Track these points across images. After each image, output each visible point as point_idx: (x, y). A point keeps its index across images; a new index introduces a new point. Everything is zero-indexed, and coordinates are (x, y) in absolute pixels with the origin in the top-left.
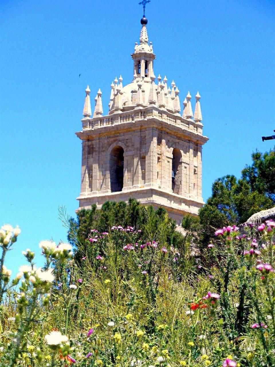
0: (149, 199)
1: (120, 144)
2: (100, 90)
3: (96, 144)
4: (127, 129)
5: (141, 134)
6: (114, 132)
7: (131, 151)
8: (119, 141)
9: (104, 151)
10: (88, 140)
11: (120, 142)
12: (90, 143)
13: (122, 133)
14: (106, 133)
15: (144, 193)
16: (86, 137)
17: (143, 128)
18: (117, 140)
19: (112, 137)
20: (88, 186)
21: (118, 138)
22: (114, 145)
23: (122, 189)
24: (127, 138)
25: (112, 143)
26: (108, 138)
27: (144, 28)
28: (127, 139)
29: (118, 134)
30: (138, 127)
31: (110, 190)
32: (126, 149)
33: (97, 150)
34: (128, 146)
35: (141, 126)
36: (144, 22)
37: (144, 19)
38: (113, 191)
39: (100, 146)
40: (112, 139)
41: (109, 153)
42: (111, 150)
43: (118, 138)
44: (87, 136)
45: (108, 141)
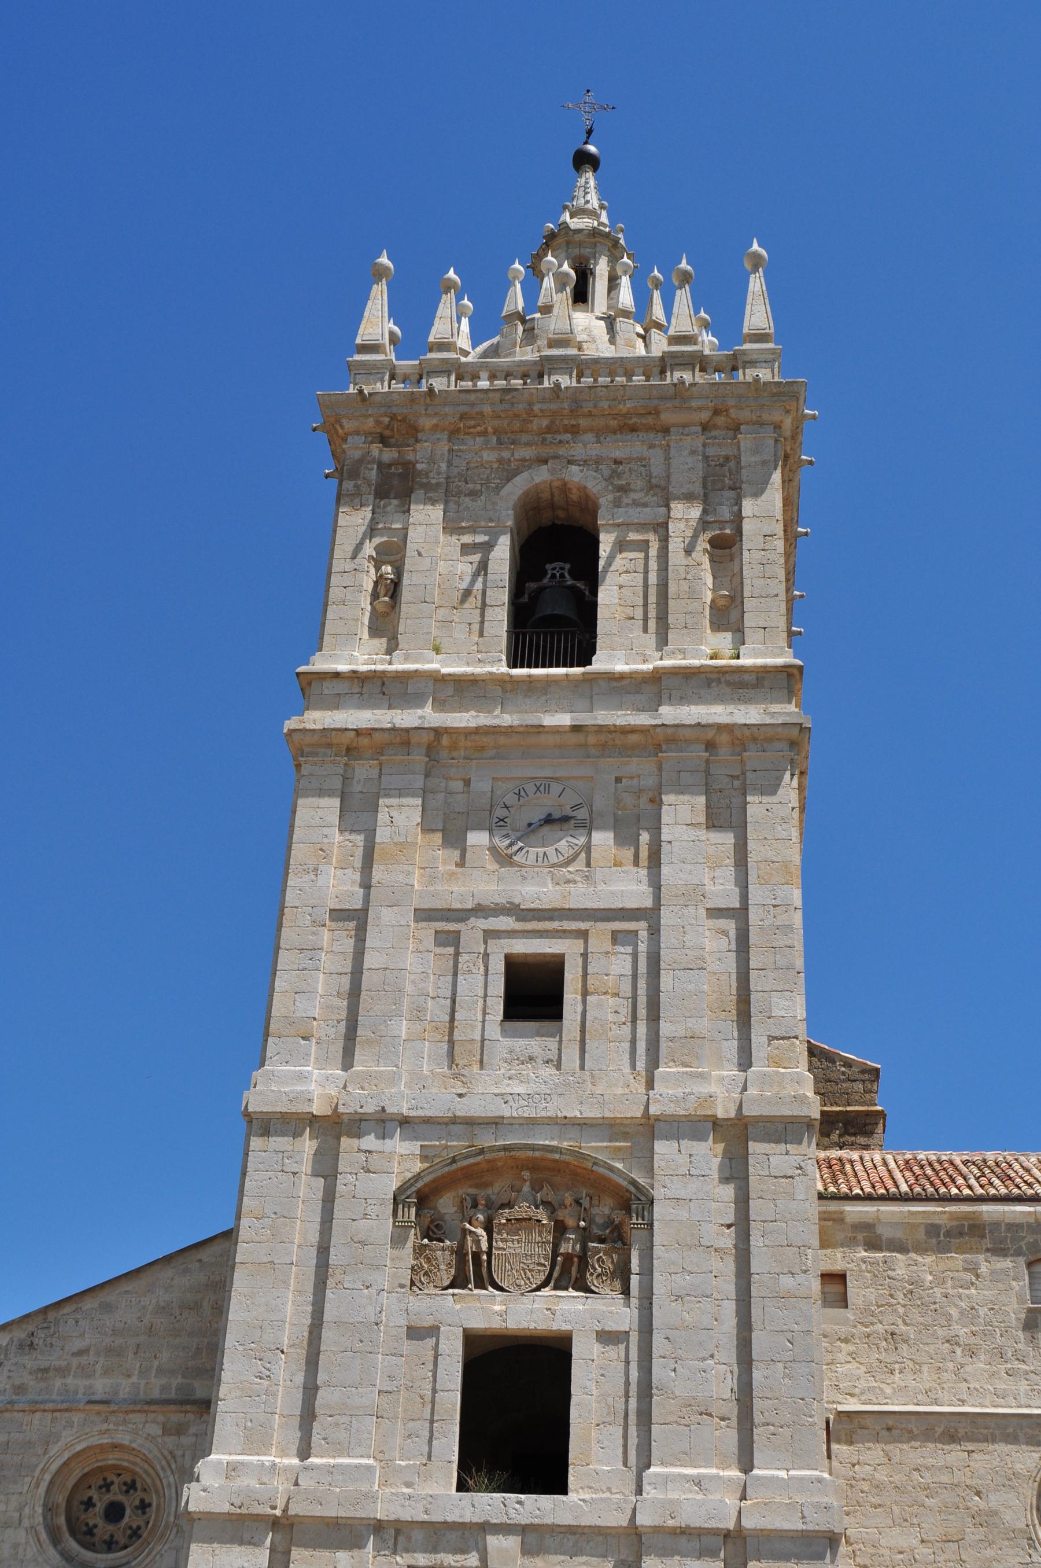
0: (776, 708)
1: (575, 475)
2: (452, 269)
3: (432, 460)
4: (628, 415)
5: (704, 445)
6: (545, 422)
7: (645, 505)
8: (570, 462)
9: (473, 494)
10: (384, 440)
11: (574, 468)
12: (389, 455)
13: (591, 430)
14: (496, 423)
15: (742, 685)
16: (378, 422)
17: (721, 420)
18: (556, 457)
19: (528, 444)
20: (366, 630)
21: (561, 451)
22: (541, 475)
23: (594, 658)
24: (618, 454)
25: (526, 464)
26: (500, 442)
27: (589, 178)
28: (618, 462)
29: (568, 436)
30: (700, 409)
31: (504, 663)
32: (610, 497)
33: (438, 484)
34: (624, 489)
35: (717, 412)
36: (583, 160)
37: (592, 148)
38: (514, 662)
39: (455, 471)
40: (527, 453)
41: (511, 504)
42: (519, 492)
43: (561, 451)
44: (386, 420)
45: (506, 454)
